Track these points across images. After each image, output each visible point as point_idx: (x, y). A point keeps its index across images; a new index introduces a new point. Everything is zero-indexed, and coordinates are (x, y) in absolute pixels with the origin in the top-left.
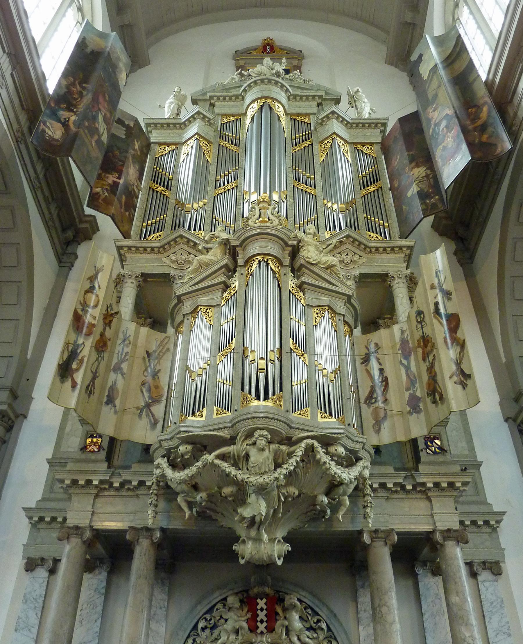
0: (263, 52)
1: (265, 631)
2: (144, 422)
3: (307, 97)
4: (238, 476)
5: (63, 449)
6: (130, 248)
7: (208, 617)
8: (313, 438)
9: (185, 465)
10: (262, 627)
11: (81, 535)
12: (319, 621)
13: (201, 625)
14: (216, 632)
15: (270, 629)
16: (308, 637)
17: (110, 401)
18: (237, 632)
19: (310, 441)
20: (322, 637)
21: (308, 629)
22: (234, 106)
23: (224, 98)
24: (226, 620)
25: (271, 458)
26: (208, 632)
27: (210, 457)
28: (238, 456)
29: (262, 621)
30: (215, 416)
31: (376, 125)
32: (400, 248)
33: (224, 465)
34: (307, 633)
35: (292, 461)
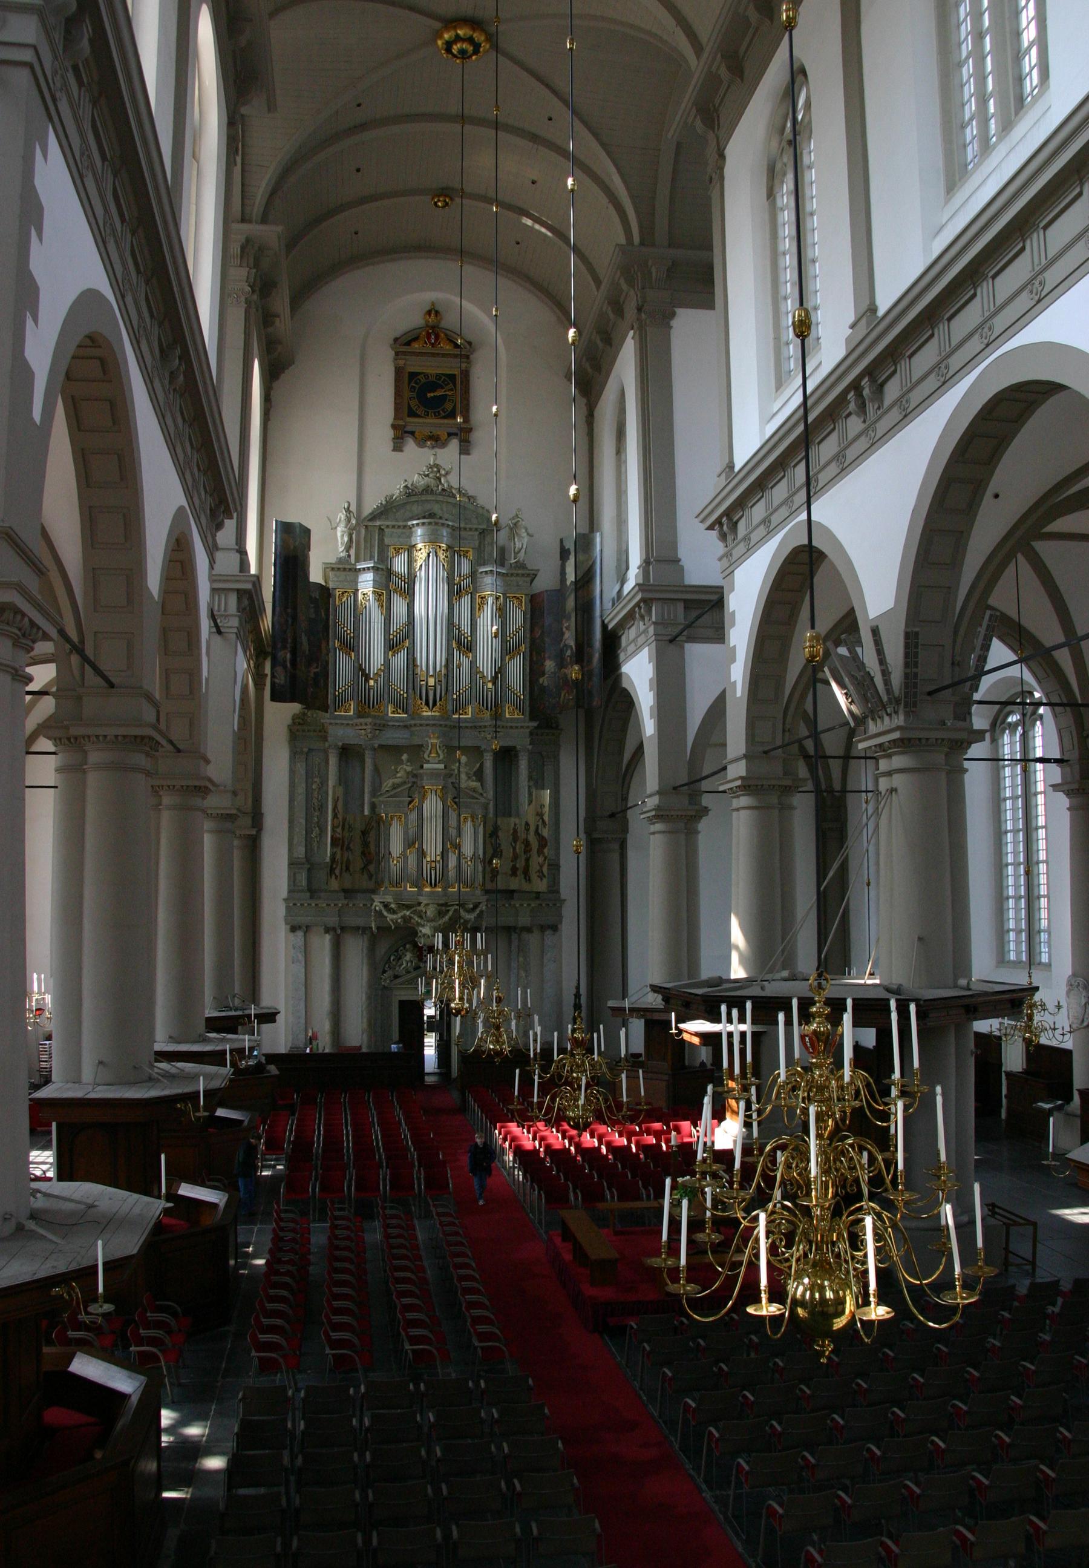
0: (426, 343)
2: (366, 876)
3: (471, 529)
5: (295, 855)
6: (331, 724)
9: (394, 912)
11: (335, 931)
17: (347, 869)
18: (412, 962)
19: (457, 907)
22: (403, 533)
23: (393, 527)
27: (408, 913)
30: (409, 889)
31: (528, 575)
32: (528, 727)
35: (447, 917)
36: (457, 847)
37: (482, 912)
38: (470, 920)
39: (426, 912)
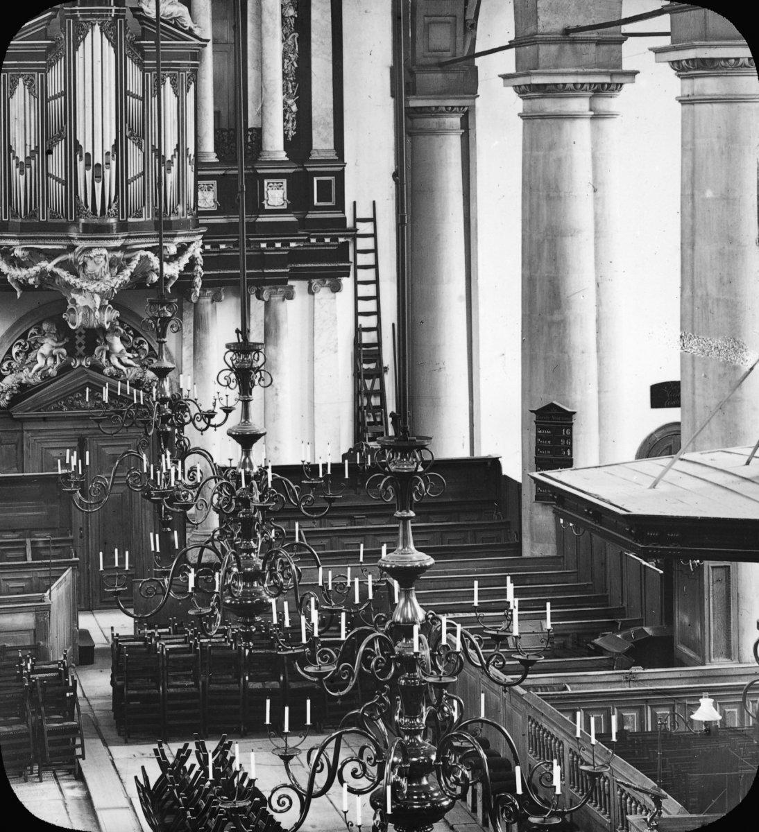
1: (84, 354)
4: (77, 285)
7: (21, 341)
8: (146, 249)
10: (81, 350)
12: (141, 342)
13: (15, 350)
14: (32, 356)
15: (89, 352)
16: (129, 358)
20: (143, 357)
21: (129, 350)
24: (42, 344)
25: (107, 264)
26: (22, 355)
27: (50, 266)
28: (76, 262)
29: (80, 345)
33: (64, 274)
34: (130, 355)
35: (127, 273)
36: (140, 137)
37: (193, 260)
38: (172, 277)
39: (85, 264)
